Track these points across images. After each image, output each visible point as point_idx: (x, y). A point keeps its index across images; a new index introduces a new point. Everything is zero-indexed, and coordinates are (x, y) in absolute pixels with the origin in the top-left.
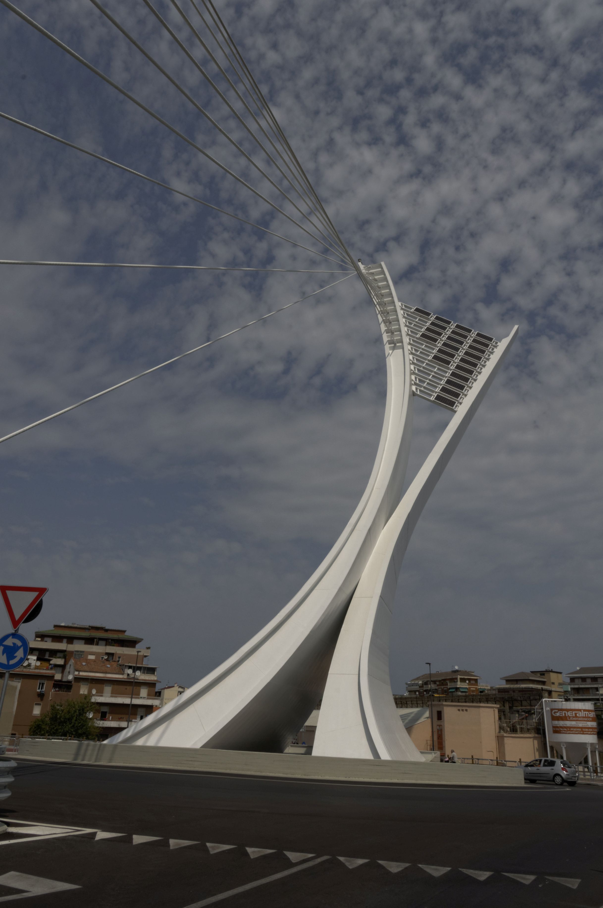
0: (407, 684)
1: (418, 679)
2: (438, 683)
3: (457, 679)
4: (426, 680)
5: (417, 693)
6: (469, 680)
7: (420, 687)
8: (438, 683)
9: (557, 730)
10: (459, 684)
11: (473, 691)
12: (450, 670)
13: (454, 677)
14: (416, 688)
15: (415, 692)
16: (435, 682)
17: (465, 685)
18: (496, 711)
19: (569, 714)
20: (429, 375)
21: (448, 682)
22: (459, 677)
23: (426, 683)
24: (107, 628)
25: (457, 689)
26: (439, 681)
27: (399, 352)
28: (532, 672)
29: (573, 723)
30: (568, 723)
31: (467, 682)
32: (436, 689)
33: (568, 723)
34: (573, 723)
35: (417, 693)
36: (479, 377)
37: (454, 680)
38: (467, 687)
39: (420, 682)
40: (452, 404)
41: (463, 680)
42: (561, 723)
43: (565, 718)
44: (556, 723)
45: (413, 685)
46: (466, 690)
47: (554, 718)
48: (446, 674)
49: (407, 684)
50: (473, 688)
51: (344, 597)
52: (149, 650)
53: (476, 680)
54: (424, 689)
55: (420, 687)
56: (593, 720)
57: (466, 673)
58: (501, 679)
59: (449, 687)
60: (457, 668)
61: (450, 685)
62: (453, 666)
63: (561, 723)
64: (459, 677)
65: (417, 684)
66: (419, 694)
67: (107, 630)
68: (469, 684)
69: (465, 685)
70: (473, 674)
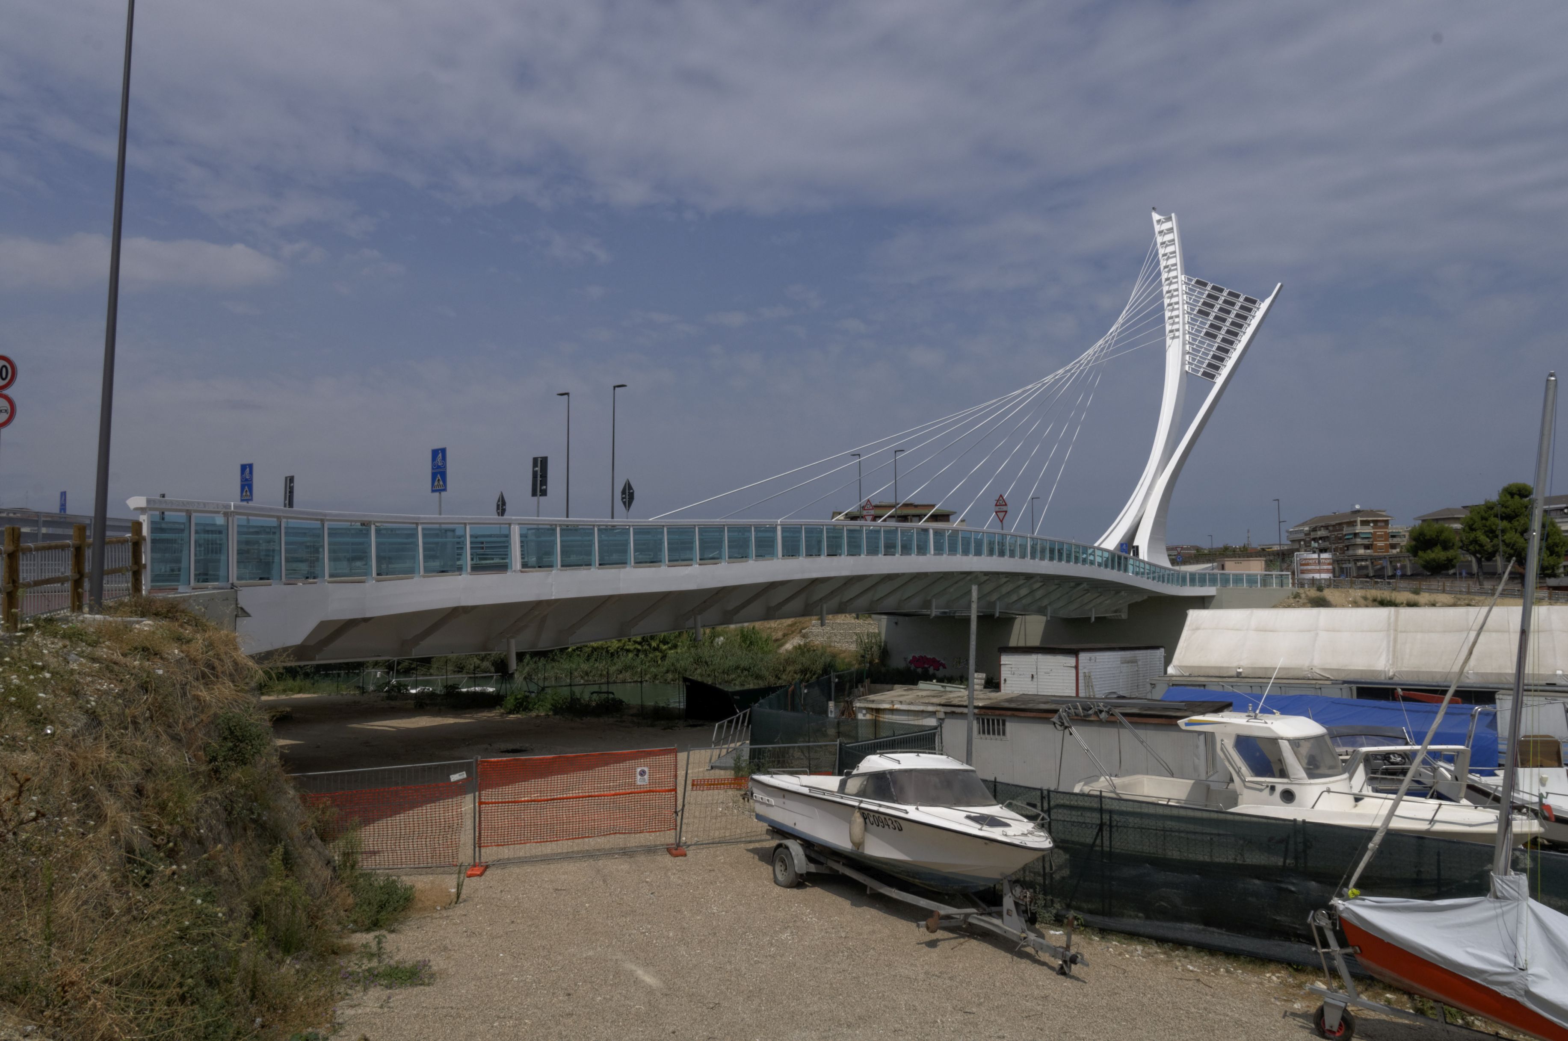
0: (1287, 532)
1: (1303, 524)
2: (1331, 528)
3: (1356, 522)
4: (1314, 526)
5: (1302, 543)
6: (1375, 522)
7: (1306, 535)
8: (1331, 528)
9: (1303, 572)
10: (1359, 529)
11: (1381, 536)
12: (1347, 510)
13: (1352, 520)
14: (1301, 536)
15: (1299, 541)
16: (1326, 527)
17: (1369, 529)
18: (1263, 563)
19: (1311, 561)
20: (1199, 351)
21: (1345, 526)
22: (1359, 519)
23: (1314, 530)
24: (916, 503)
25: (1356, 535)
26: (1334, 526)
27: (1176, 340)
28: (1464, 507)
29: (1313, 567)
30: (1309, 567)
31: (1372, 525)
32: (1327, 537)
33: (1309, 567)
34: (1313, 567)
35: (1302, 543)
36: (1253, 321)
37: (1352, 524)
38: (1372, 531)
39: (1307, 529)
40: (1212, 377)
41: (1365, 523)
42: (1305, 567)
43: (1308, 564)
44: (1302, 567)
45: (1296, 532)
46: (1370, 536)
47: (1302, 565)
48: (1344, 515)
49: (1287, 532)
50: (1380, 532)
51: (1137, 519)
52: (964, 523)
53: (1387, 522)
54: (1312, 537)
55: (1306, 535)
56: (1329, 564)
57: (1372, 513)
58: (1416, 519)
59: (1344, 533)
60: (1357, 507)
61: (1346, 530)
62: (1353, 505)
63: (1305, 567)
64: (1359, 519)
65: (1302, 531)
66: (1305, 543)
67: (916, 506)
68: (1373, 528)
69: (1369, 529)
70: (1384, 513)
